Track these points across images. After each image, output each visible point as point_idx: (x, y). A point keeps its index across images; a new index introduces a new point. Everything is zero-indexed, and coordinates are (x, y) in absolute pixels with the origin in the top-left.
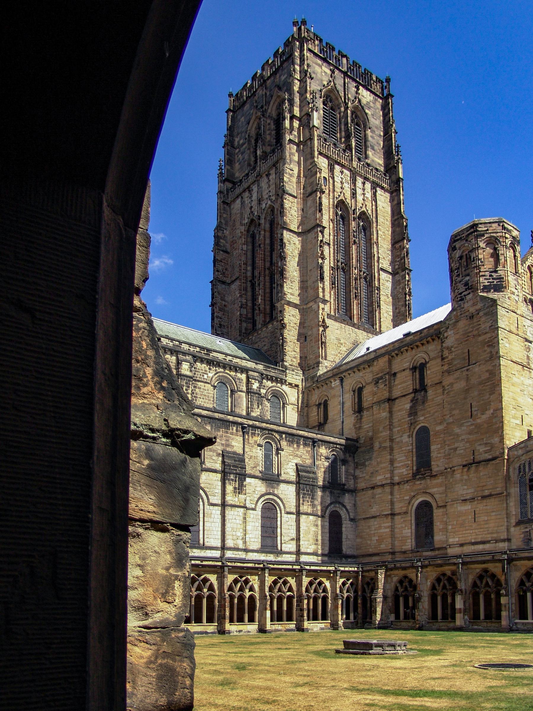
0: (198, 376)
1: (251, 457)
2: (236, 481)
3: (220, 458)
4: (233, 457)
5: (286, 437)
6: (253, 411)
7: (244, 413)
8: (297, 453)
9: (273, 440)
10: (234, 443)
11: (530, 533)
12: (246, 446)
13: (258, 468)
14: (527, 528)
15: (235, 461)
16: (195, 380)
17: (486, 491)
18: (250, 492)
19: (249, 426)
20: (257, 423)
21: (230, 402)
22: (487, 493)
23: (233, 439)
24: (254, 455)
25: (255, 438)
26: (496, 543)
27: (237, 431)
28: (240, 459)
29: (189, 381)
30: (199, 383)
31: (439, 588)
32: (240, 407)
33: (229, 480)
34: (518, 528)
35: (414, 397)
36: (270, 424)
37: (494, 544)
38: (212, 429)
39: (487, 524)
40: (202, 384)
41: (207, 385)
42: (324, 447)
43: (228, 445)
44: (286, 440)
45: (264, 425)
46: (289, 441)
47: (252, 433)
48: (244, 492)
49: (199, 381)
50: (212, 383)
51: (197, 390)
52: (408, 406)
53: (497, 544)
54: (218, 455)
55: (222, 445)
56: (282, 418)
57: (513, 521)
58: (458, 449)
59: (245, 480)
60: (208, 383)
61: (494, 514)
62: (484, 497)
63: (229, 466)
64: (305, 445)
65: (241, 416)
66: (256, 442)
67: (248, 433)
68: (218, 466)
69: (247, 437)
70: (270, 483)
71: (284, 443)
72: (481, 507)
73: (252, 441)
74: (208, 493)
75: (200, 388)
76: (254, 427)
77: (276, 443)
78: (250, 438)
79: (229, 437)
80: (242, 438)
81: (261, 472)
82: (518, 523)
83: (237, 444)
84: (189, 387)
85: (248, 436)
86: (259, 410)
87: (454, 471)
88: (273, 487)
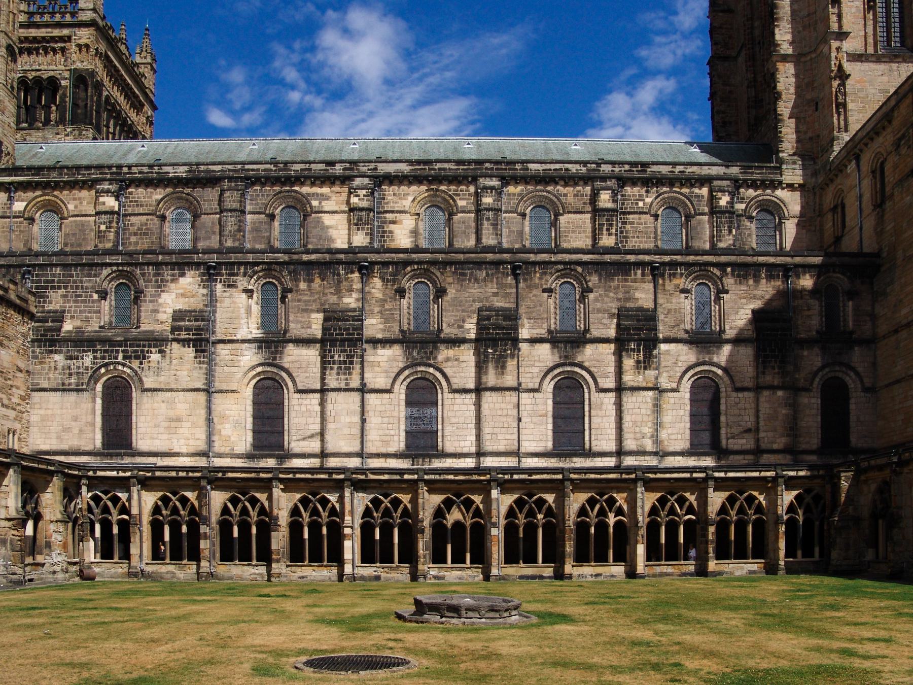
0: (628, 206)
1: (669, 311)
2: (639, 351)
3: (615, 321)
4: (635, 316)
5: (733, 271)
6: (720, 241)
7: (707, 246)
8: (755, 292)
9: (710, 278)
10: (638, 295)
12: (659, 296)
13: (682, 326)
15: (638, 320)
16: (624, 213)
18: (669, 364)
19: (663, 264)
20: (678, 258)
21: (684, 234)
23: (636, 289)
24: (673, 307)
25: (676, 281)
27: (643, 274)
28: (649, 318)
29: (612, 216)
30: (631, 217)
32: (701, 238)
33: (627, 351)
36: (702, 255)
38: (600, 280)
40: (636, 216)
41: (644, 216)
42: (808, 276)
43: (627, 300)
44: (733, 275)
45: (691, 258)
46: (739, 276)
47: (670, 275)
48: (654, 366)
49: (629, 213)
50: (652, 212)
51: (628, 227)
54: (612, 316)
55: (619, 300)
56: (778, 242)
59: (655, 347)
60: (645, 213)
63: (627, 329)
64: (770, 277)
65: (705, 253)
66: (677, 286)
67: (663, 276)
68: (612, 333)
69: (661, 282)
70: (705, 348)
71: (729, 282)
73: (669, 286)
74: (596, 375)
75: (632, 223)
76: (673, 265)
77: (715, 284)
78: (667, 282)
79: (630, 286)
80: (652, 285)
81: (687, 332)
83: (643, 296)
84: (611, 225)
85: (664, 280)
86: (731, 237)
88: (709, 353)
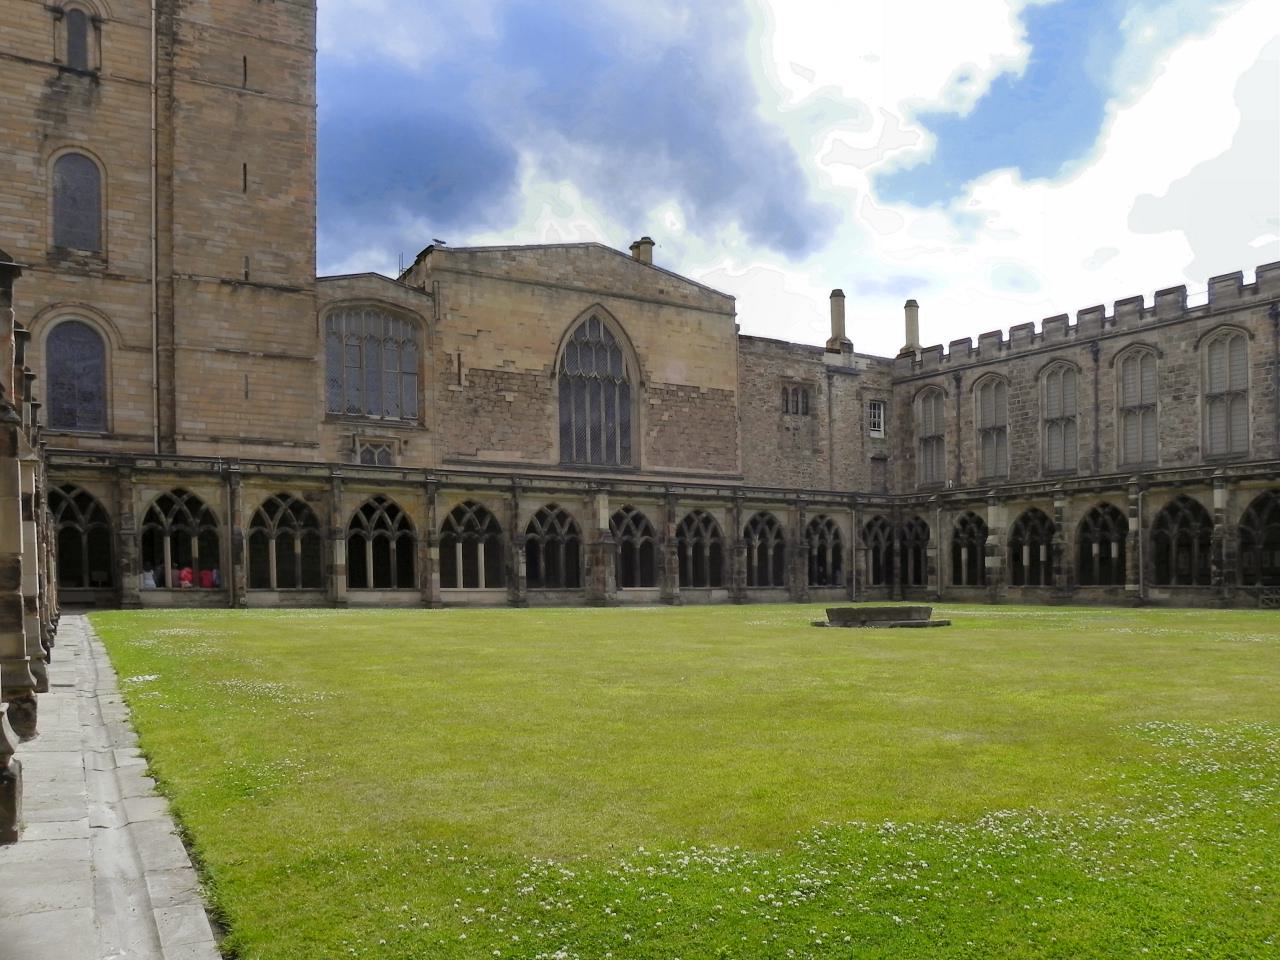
11: (354, 440)
14: (348, 430)
17: (275, 345)
22: (275, 348)
26: (295, 446)
31: (272, 528)
34: (330, 428)
35: (59, 78)
37: (290, 450)
39: (275, 408)
52: (38, 90)
53: (297, 450)
57: (321, 412)
58: (208, 242)
61: (290, 392)
62: (268, 356)
72: (265, 369)
82: (330, 419)
87: (197, 283)
